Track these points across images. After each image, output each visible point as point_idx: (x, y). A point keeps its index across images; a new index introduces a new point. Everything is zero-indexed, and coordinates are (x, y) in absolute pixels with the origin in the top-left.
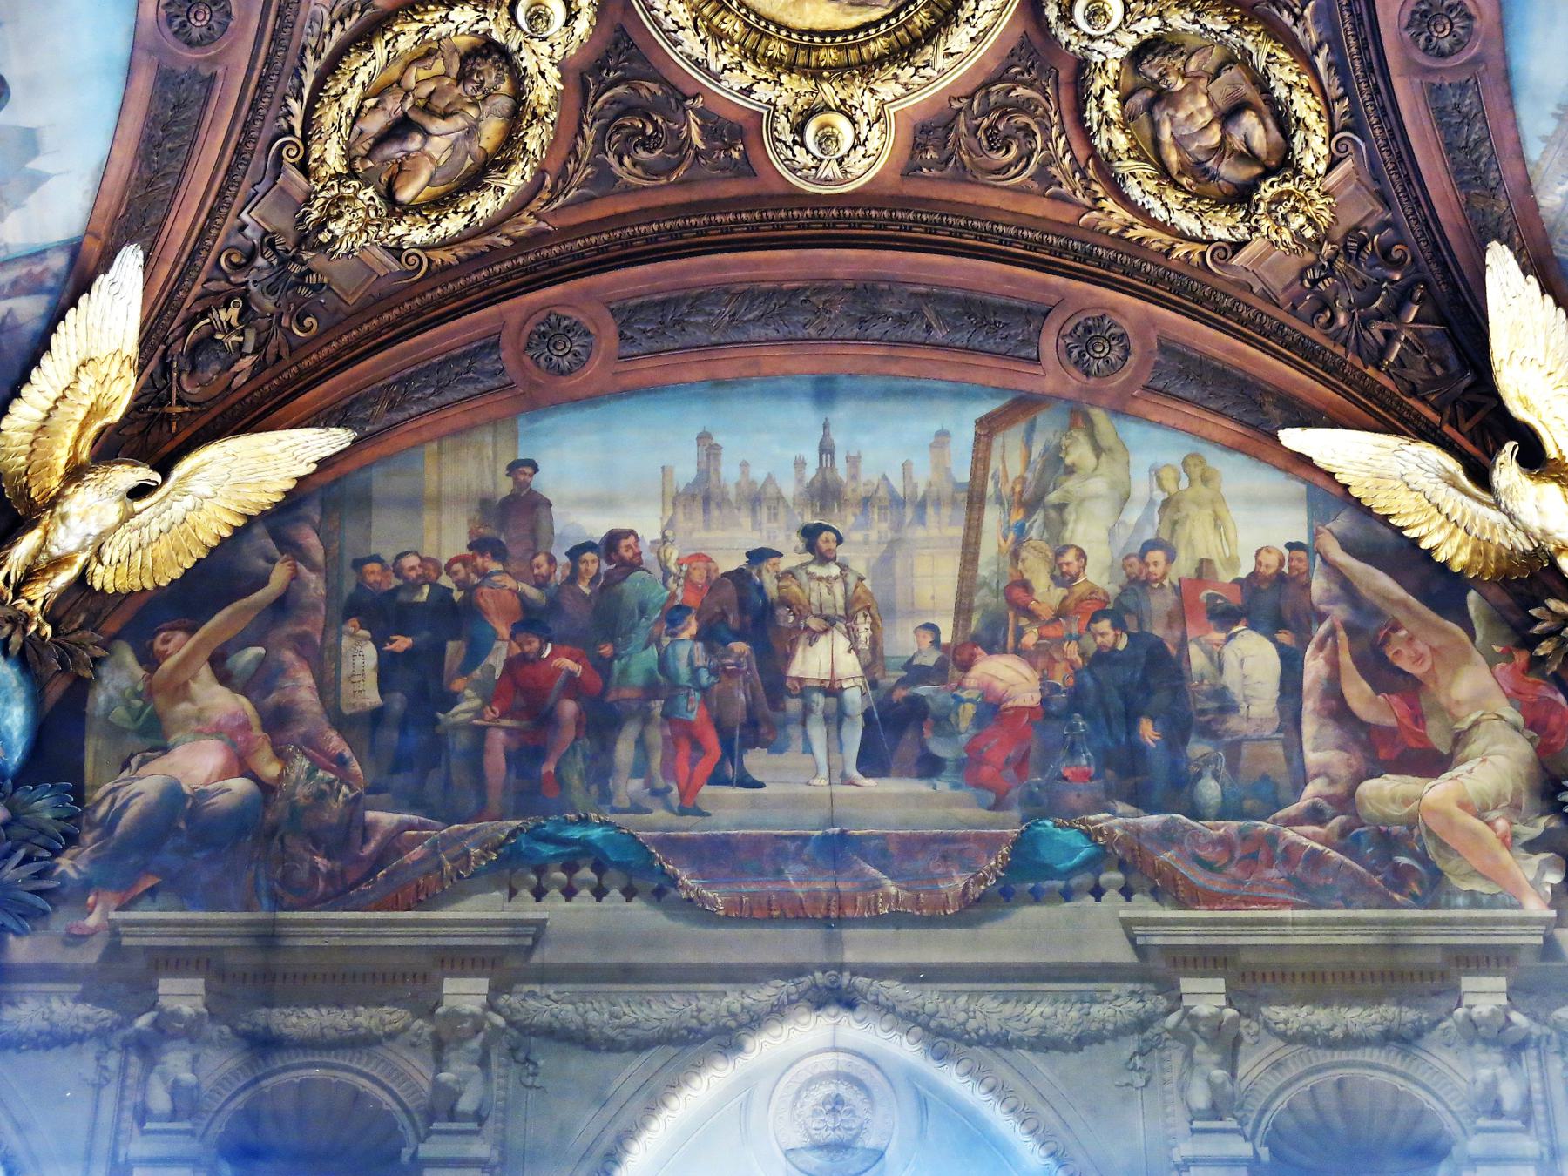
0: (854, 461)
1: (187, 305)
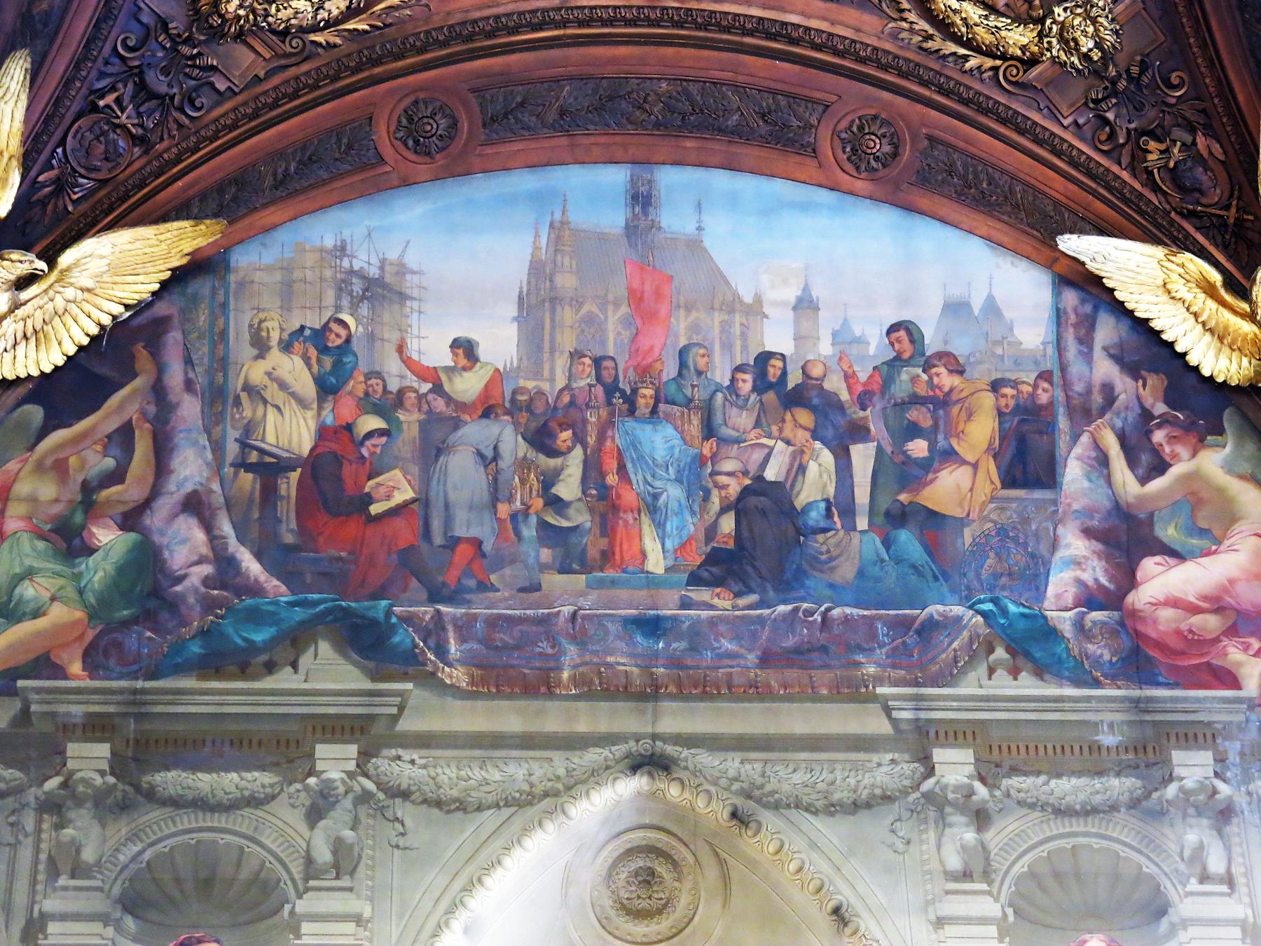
1: (1137, 186)
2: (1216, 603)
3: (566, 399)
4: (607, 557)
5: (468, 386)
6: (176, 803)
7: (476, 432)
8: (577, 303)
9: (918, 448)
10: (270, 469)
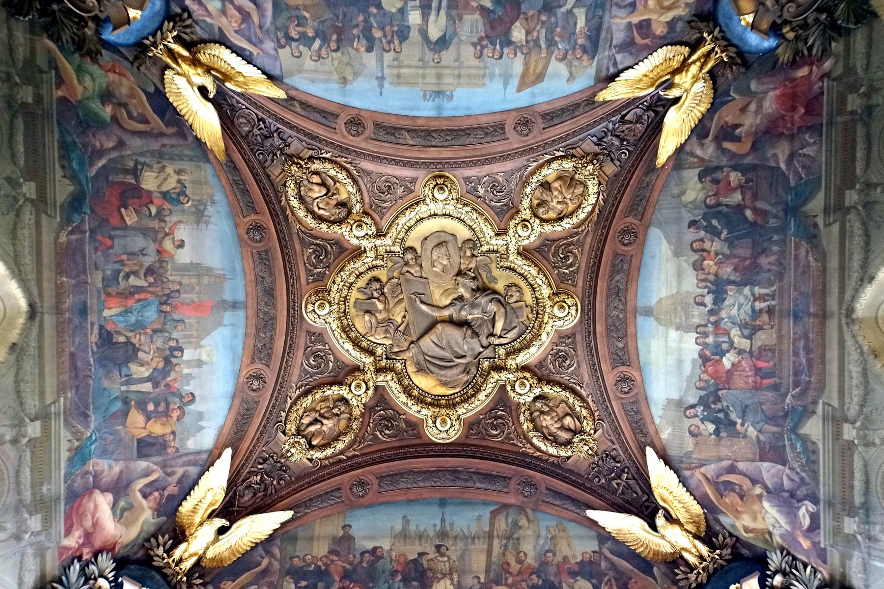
0: (452, 525)
2: (95, 524)
3: (165, 280)
4: (109, 295)
5: (168, 245)
6: (11, 127)
7: (152, 247)
8: (199, 284)
9: (151, 407)
10: (136, 173)
